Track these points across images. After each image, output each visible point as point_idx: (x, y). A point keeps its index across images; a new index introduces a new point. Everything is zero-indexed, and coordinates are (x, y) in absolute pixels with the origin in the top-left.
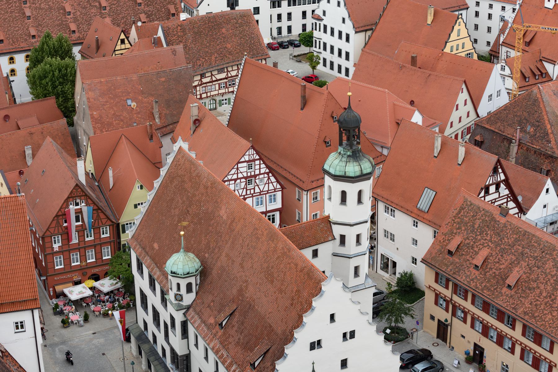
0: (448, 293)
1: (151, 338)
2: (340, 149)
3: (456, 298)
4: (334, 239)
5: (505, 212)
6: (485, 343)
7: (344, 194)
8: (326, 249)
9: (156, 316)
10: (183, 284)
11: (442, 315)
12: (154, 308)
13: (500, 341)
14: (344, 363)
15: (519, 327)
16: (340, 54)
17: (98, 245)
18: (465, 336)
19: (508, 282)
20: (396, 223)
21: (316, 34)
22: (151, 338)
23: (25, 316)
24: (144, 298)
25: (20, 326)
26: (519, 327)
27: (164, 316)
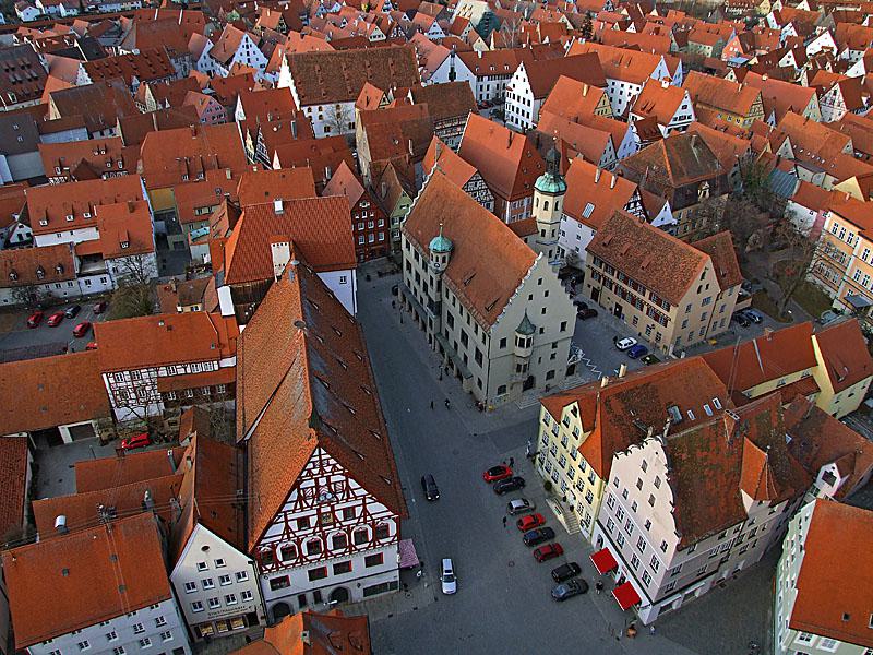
2: (546, 174)
3: (606, 274)
6: (623, 303)
7: (546, 203)
11: (596, 284)
13: (634, 301)
15: (648, 293)
16: (523, 114)
17: (376, 231)
18: (610, 298)
19: (642, 265)
20: (569, 224)
21: (507, 99)
25: (344, 279)
26: (648, 293)
27: (425, 277)
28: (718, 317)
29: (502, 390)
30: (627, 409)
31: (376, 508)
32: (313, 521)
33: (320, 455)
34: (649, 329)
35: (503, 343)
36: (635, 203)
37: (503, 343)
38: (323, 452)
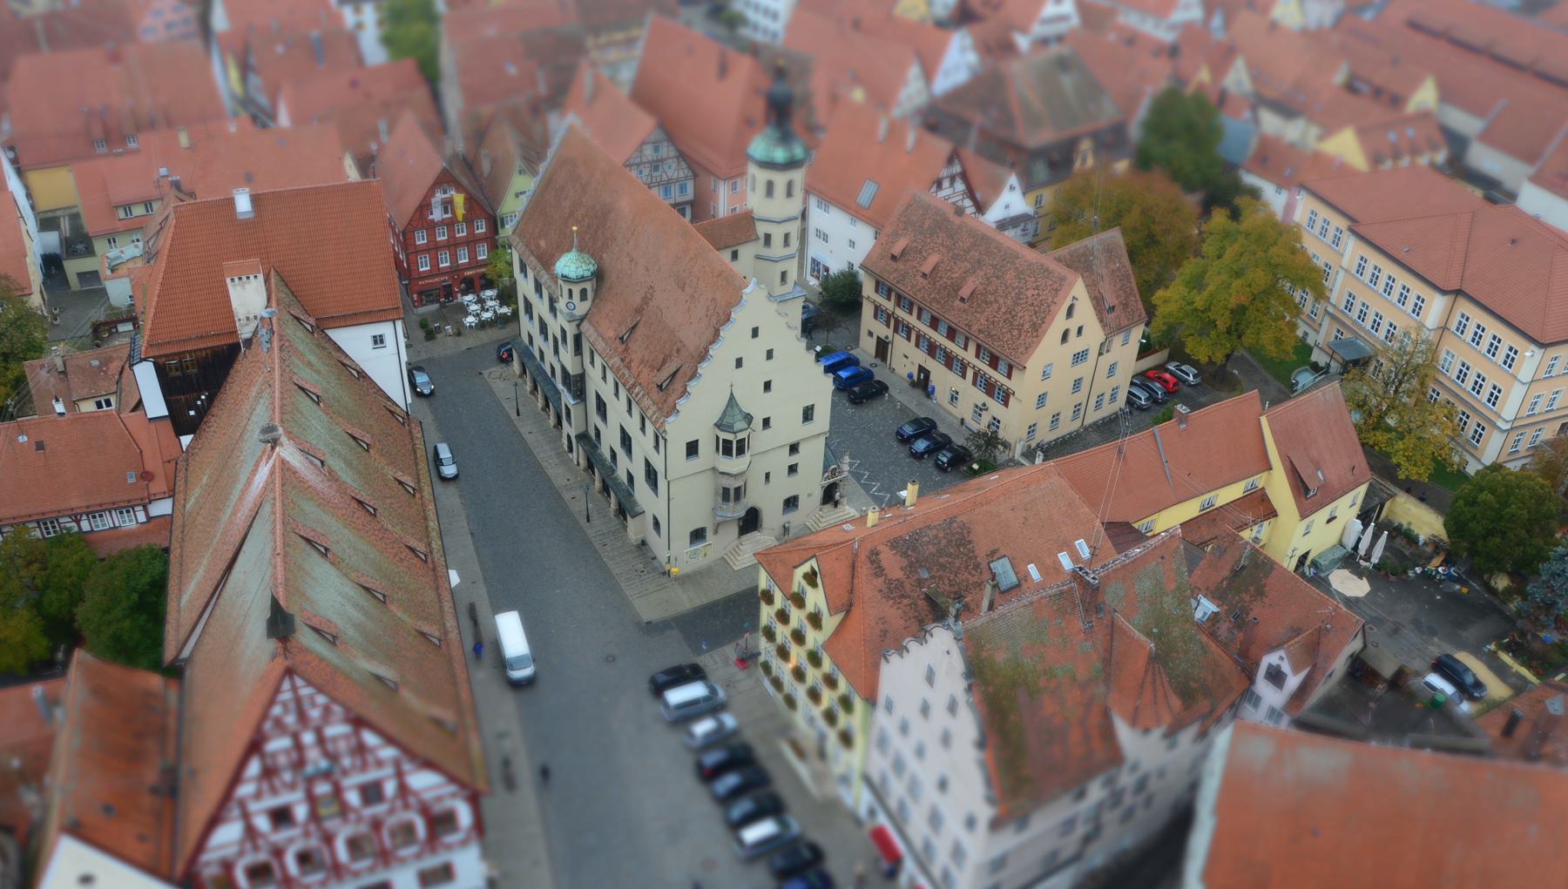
0: (889, 305)
1: (537, 355)
4: (758, 239)
5: (960, 211)
8: (747, 252)
9: (543, 328)
10: (576, 290)
11: (882, 330)
12: (541, 319)
13: (949, 361)
14: (767, 386)
15: (972, 348)
20: (827, 219)
22: (537, 355)
23: (385, 329)
24: (529, 307)
25: (378, 340)
27: (554, 328)
28: (1103, 385)
29: (698, 535)
30: (911, 568)
31: (423, 781)
32: (301, 812)
33: (294, 689)
34: (980, 409)
35: (692, 449)
36: (952, 179)
37: (692, 449)
38: (299, 682)
